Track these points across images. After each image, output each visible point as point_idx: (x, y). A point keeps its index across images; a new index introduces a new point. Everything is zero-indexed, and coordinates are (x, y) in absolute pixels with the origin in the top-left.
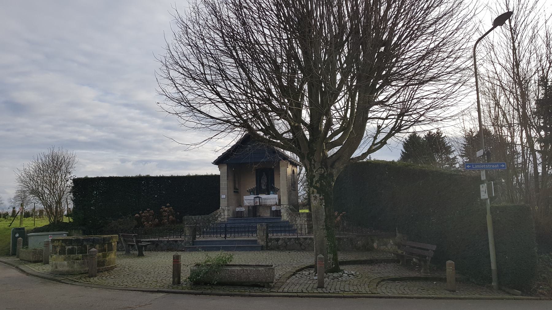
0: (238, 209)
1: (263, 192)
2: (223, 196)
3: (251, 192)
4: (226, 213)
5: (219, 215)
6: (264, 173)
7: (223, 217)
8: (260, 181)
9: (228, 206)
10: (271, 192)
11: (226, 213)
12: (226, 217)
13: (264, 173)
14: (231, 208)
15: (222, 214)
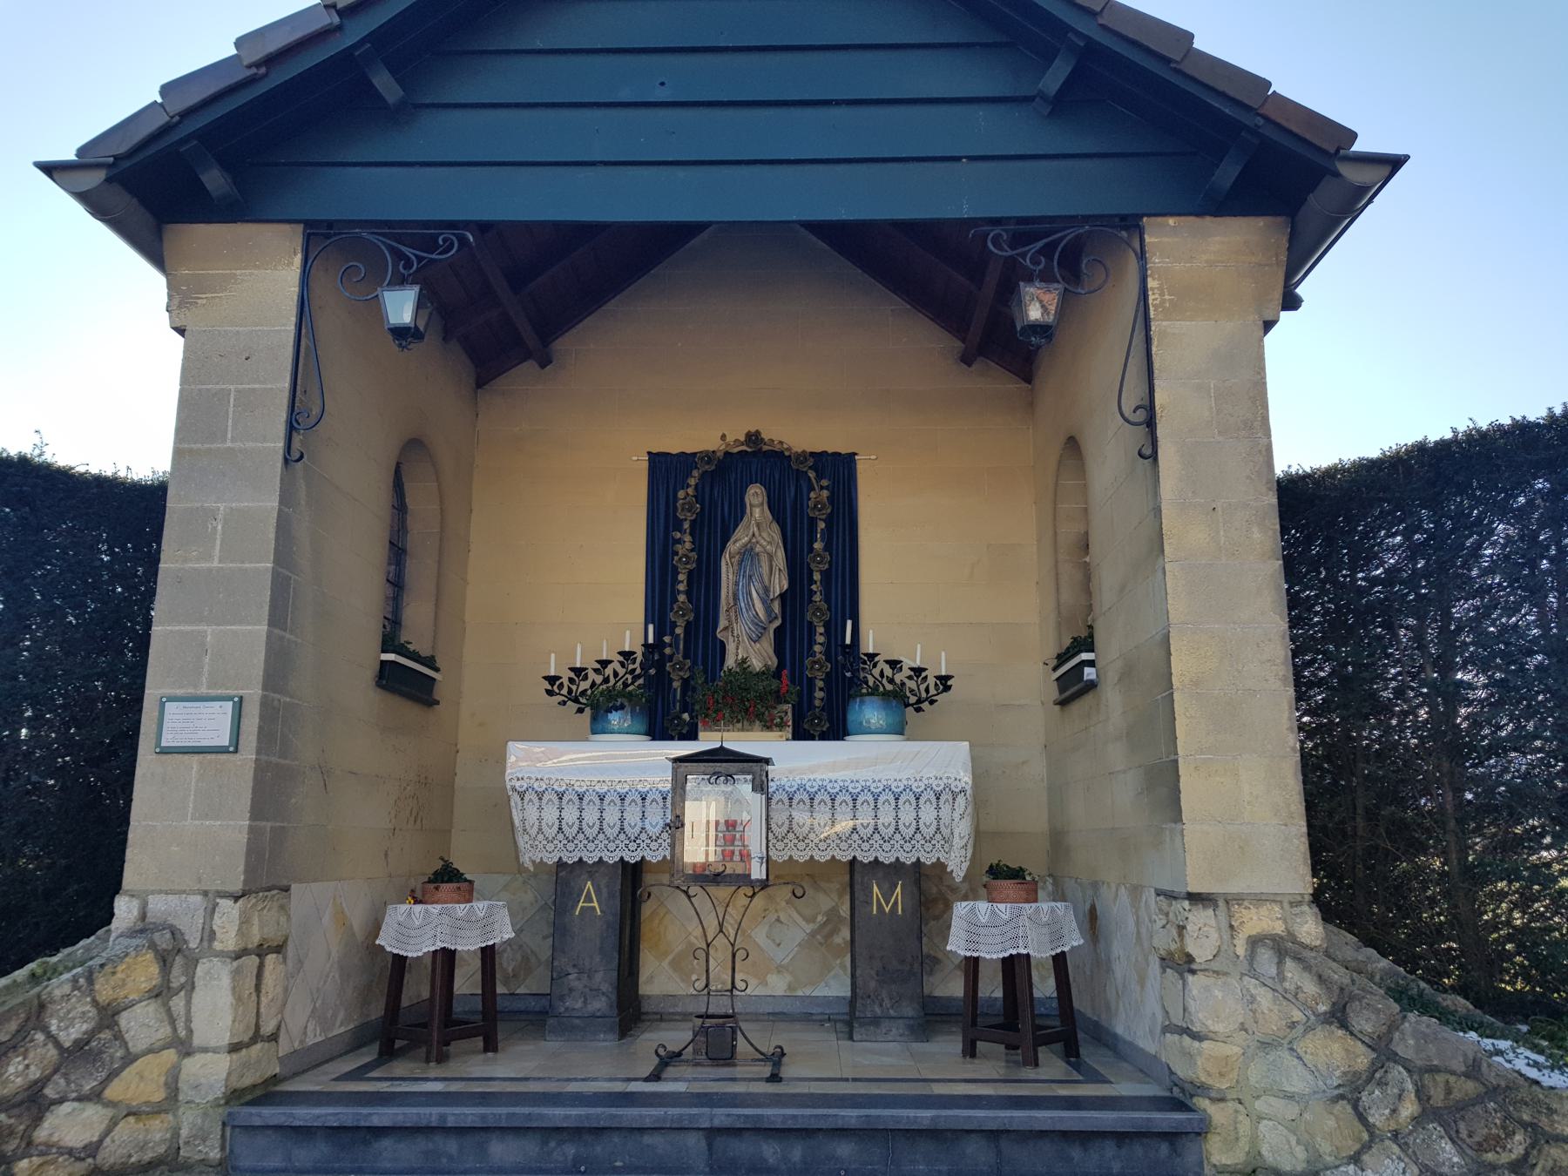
0: (416, 931)
1: (748, 702)
2: (208, 723)
3: (593, 699)
4: (215, 1006)
5: (79, 1053)
6: (755, 496)
7: (139, 1084)
8: (706, 580)
9: (266, 877)
10: (871, 713)
11: (215, 1006)
12: (210, 1073)
13: (755, 496)
14: (322, 913)
15: (142, 1024)
